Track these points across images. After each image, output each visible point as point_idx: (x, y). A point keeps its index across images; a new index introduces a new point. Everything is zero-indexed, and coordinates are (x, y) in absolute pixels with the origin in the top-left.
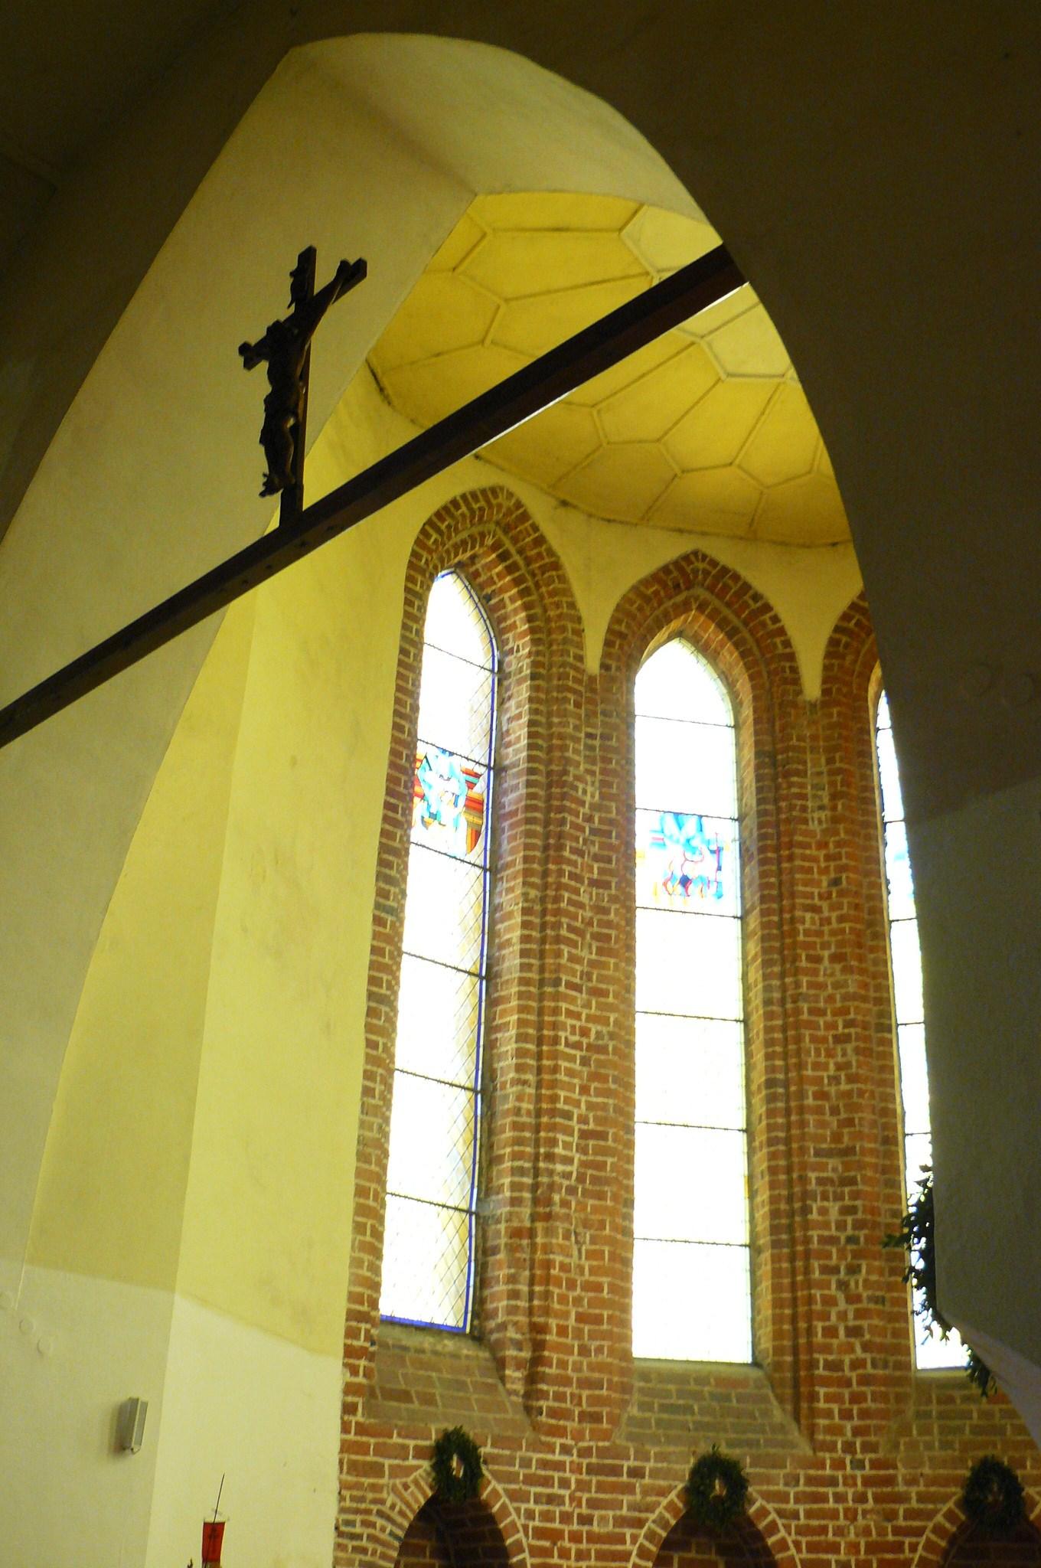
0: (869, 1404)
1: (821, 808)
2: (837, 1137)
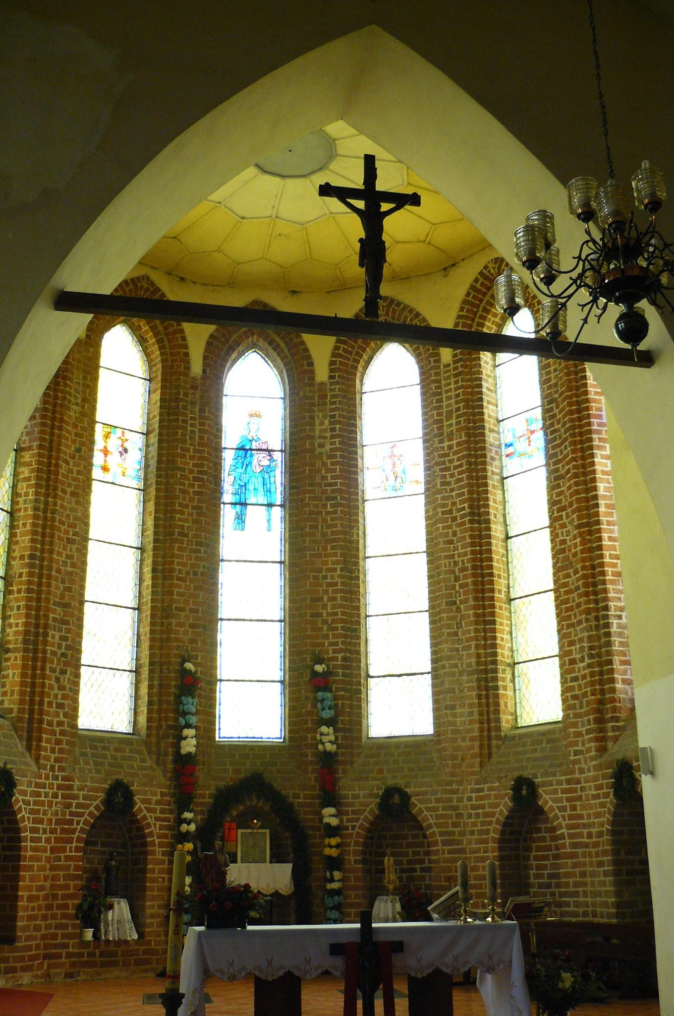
0: (64, 746)
1: (77, 404)
2: (62, 597)
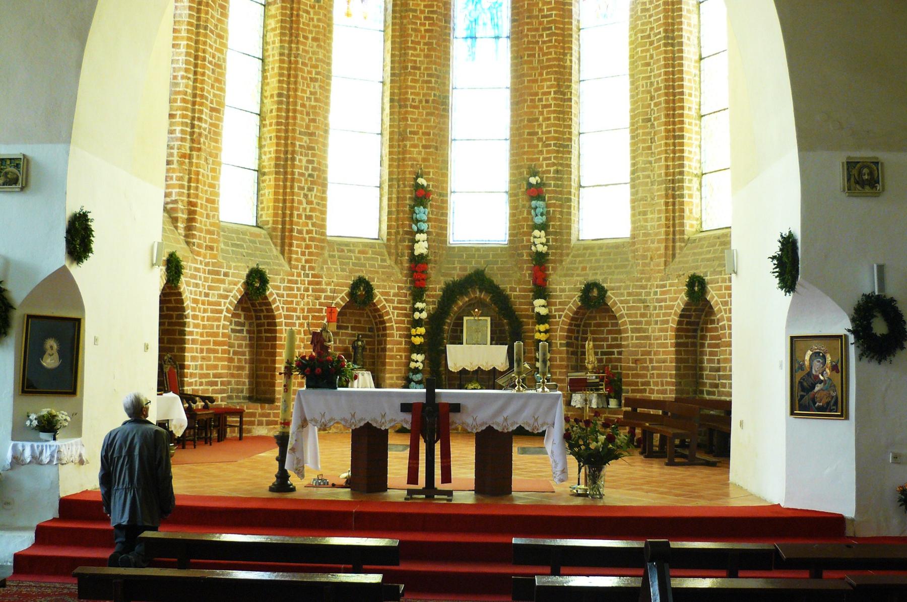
0: (313, 250)
